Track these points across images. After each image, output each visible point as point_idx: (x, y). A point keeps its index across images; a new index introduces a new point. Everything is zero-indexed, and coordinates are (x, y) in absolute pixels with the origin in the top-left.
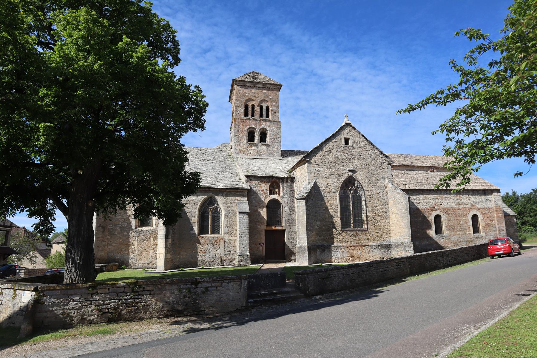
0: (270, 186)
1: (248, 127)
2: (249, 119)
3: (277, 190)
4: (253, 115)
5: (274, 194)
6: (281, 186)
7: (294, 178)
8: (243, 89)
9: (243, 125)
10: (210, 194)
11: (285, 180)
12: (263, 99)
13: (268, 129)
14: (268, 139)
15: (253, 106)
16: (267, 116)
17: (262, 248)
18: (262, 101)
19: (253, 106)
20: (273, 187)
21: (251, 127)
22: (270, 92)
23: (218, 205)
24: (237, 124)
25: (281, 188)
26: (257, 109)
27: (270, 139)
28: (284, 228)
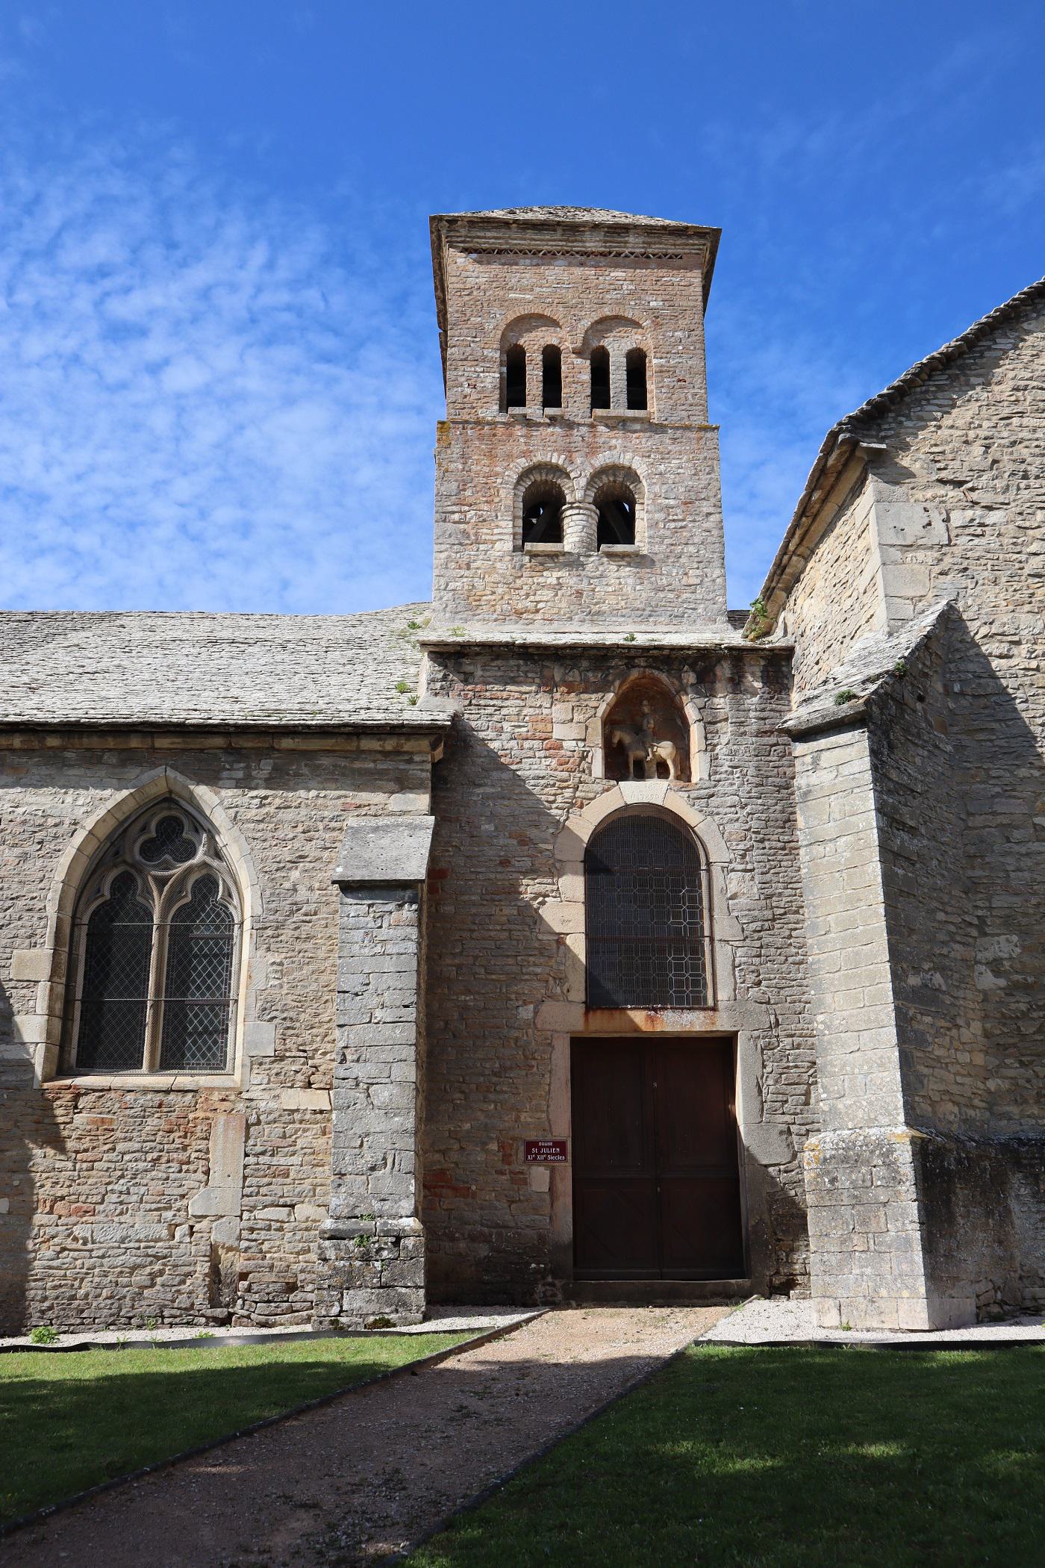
0: (610, 723)
1: (523, 463)
2: (528, 422)
3: (665, 750)
4: (552, 395)
5: (641, 775)
6: (691, 712)
7: (789, 651)
8: (495, 268)
9: (491, 455)
10: (159, 778)
11: (724, 670)
12: (607, 311)
13: (640, 467)
14: (641, 526)
15: (552, 358)
16: (637, 398)
17: (550, 1184)
18: (606, 324)
19: (552, 358)
20: (638, 730)
22: (647, 275)
23: (218, 855)
24: (456, 449)
25: (696, 732)
26: (576, 373)
27: (653, 525)
28: (722, 1023)
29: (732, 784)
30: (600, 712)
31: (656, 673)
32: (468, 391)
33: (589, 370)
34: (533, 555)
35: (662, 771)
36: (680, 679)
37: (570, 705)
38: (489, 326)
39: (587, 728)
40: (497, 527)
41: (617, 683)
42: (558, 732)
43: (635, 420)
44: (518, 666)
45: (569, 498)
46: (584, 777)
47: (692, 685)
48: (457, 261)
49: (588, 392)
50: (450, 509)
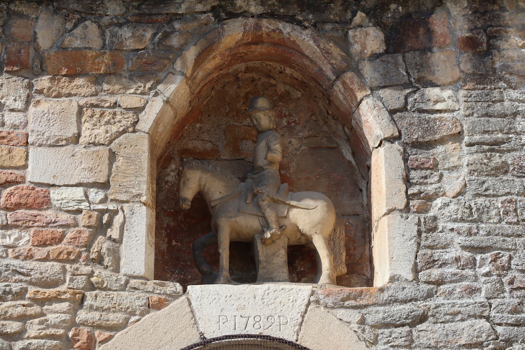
0: (171, 157)
3: (310, 216)
5: (246, 266)
6: (373, 120)
20: (247, 171)
25: (384, 169)
29: (472, 291)
30: (147, 120)
31: (286, 29)
35: (301, 262)
36: (344, 43)
37: (74, 103)
39: (113, 156)
41: (191, 54)
42: (40, 166)
46: (100, 274)
47: (375, 57)
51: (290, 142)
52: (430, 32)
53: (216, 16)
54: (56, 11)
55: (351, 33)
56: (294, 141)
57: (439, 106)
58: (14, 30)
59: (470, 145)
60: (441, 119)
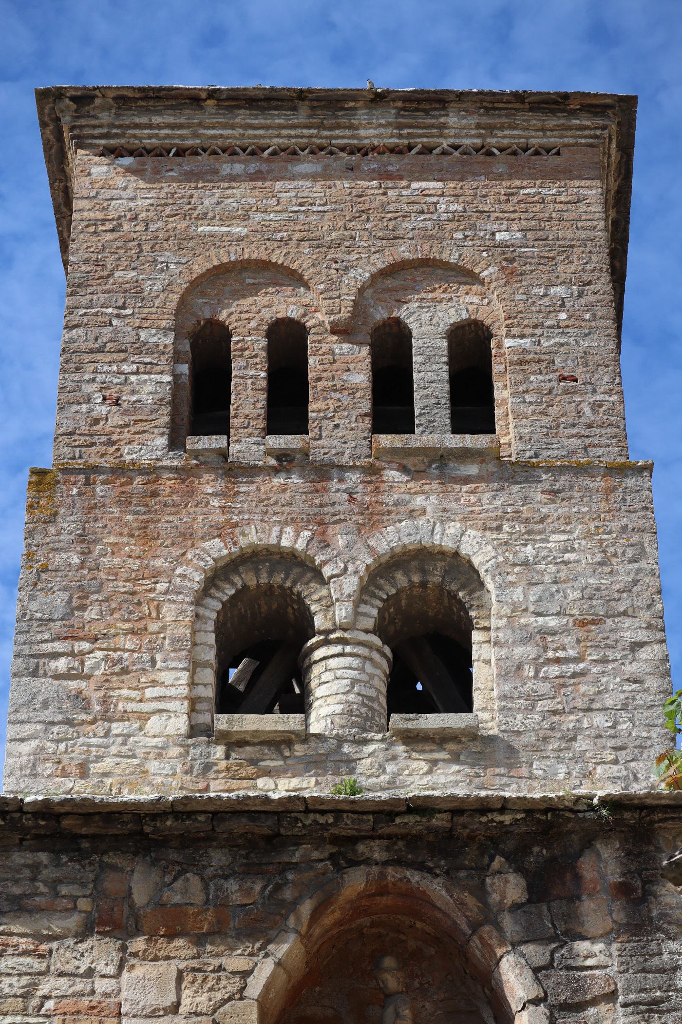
1: (218, 548)
2: (231, 470)
6: (515, 980)
9: (145, 535)
11: (604, 865)
12: (404, 252)
13: (480, 551)
14: (483, 675)
15: (287, 346)
18: (400, 277)
19: (287, 346)
21: (253, 558)
22: (491, 192)
24: (68, 524)
26: (341, 373)
27: (511, 671)
30: (256, 986)
31: (415, 877)
32: (103, 410)
33: (367, 364)
34: (234, 743)
36: (481, 892)
37: (170, 969)
38: (153, 286)
40: (154, 683)
41: (306, 908)
43: (465, 455)
44: (35, 868)
45: (319, 622)
47: (515, 907)
48: (92, 171)
49: (366, 406)
50: (48, 647)
51: (423, 1006)
52: (578, 878)
53: (335, 864)
54: (154, 863)
55: (488, 880)
56: (427, 1004)
57: (589, 962)
58: (107, 885)
59: (625, 1005)
60: (592, 977)
